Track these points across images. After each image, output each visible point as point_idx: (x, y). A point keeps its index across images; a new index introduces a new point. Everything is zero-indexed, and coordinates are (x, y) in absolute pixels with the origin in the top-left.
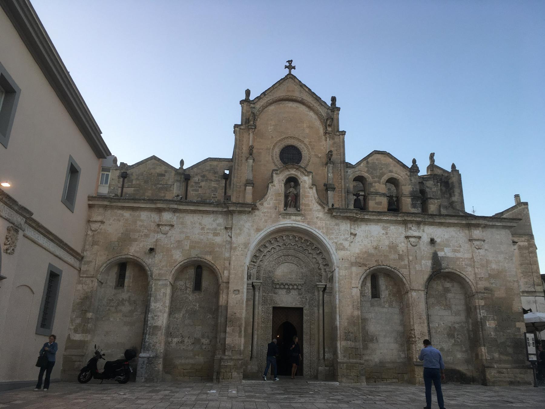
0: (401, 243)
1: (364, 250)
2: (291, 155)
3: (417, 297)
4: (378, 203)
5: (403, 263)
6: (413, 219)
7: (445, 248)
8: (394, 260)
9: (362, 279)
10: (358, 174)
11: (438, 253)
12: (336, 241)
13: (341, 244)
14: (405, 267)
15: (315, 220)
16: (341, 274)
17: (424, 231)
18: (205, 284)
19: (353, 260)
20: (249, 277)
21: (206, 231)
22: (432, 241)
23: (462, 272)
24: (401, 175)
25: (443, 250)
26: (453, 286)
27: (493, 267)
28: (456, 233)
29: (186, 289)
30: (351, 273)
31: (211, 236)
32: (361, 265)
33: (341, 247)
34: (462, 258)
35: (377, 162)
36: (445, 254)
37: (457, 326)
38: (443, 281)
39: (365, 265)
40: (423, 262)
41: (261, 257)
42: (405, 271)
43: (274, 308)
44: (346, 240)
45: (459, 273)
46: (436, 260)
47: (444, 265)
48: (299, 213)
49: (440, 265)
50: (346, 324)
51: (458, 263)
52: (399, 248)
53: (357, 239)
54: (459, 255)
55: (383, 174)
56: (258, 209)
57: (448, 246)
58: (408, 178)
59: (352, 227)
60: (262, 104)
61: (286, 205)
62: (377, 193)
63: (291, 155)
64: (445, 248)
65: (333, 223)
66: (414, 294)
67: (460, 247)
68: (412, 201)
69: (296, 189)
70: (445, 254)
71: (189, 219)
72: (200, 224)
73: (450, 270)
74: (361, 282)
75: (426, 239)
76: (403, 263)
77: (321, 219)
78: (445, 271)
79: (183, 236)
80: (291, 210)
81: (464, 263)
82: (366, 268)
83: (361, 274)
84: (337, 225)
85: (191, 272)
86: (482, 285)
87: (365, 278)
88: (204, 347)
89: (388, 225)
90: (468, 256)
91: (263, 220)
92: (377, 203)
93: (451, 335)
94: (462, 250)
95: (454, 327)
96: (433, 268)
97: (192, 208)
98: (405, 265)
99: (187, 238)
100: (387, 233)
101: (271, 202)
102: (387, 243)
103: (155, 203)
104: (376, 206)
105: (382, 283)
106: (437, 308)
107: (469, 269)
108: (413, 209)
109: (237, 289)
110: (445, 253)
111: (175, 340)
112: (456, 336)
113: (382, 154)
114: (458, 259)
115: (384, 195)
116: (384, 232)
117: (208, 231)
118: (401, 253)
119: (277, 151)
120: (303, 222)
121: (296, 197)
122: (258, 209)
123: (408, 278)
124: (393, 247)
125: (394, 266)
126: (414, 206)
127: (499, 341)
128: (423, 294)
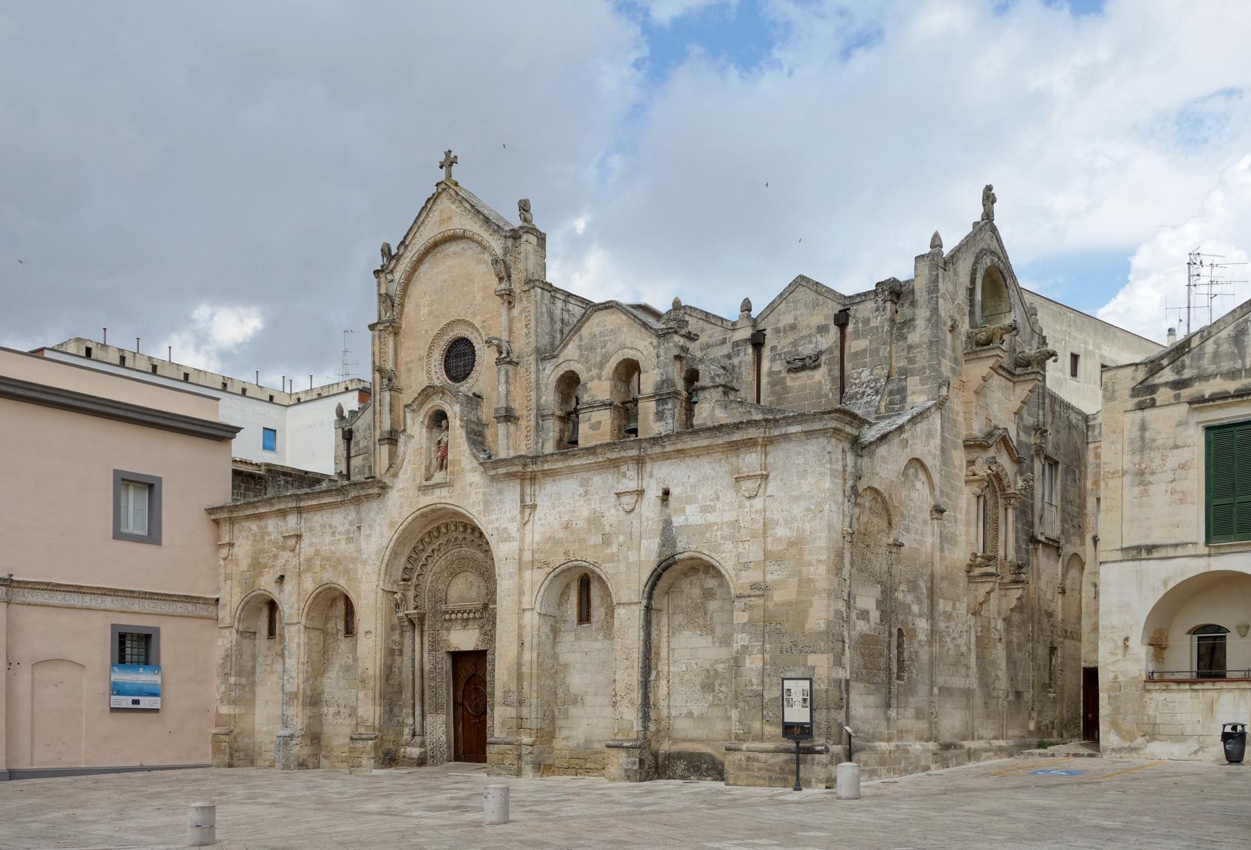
0: (609, 510)
1: (548, 534)
5: (609, 551)
6: (623, 454)
7: (688, 507)
8: (595, 546)
11: (673, 519)
12: (497, 525)
13: (505, 529)
14: (612, 559)
17: (651, 476)
22: (666, 493)
23: (713, 555)
24: (641, 346)
25: (683, 510)
27: (779, 534)
28: (713, 469)
31: (343, 545)
34: (716, 524)
35: (596, 330)
36: (686, 519)
38: (703, 576)
44: (513, 520)
45: (708, 559)
46: (667, 533)
47: (680, 546)
49: (675, 546)
51: (708, 535)
52: (605, 522)
53: (539, 513)
54: (711, 518)
55: (606, 358)
56: (389, 487)
57: (690, 500)
58: (654, 352)
59: (528, 491)
64: (688, 507)
65: (495, 491)
67: (718, 498)
68: (658, 405)
70: (686, 519)
71: (318, 519)
72: (330, 526)
73: (691, 554)
75: (653, 493)
76: (609, 551)
78: (681, 556)
81: (719, 533)
86: (753, 576)
89: (589, 475)
90: (729, 517)
92: (593, 427)
94: (719, 504)
96: (660, 554)
97: (314, 502)
98: (613, 554)
100: (586, 492)
102: (585, 513)
103: (257, 508)
104: (591, 431)
106: (687, 633)
107: (729, 546)
108: (659, 424)
110: (687, 516)
113: (607, 308)
114: (710, 526)
116: (581, 491)
118: (607, 529)
122: (389, 487)
124: (595, 521)
126: (660, 416)
127: (767, 696)
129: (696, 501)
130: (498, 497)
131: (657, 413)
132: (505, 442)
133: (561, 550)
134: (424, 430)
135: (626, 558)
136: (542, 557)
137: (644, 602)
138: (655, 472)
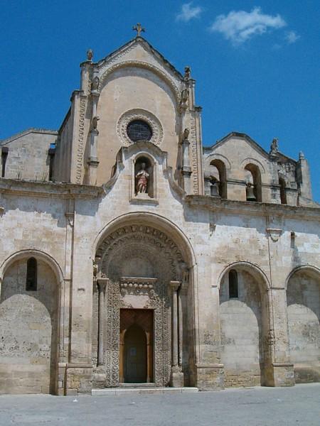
1: (224, 245)
2: (140, 128)
3: (277, 298)
4: (236, 193)
5: (263, 259)
7: (305, 244)
8: (254, 255)
9: (221, 277)
10: (215, 157)
15: (171, 209)
16: (199, 271)
17: (284, 225)
18: (40, 281)
19: (213, 255)
20: (95, 274)
21: (42, 218)
26: (309, 284)
29: (18, 287)
30: (211, 270)
32: (220, 261)
33: (200, 241)
36: (305, 249)
37: (312, 324)
38: (300, 278)
39: (225, 262)
40: (284, 258)
41: (107, 250)
42: (265, 269)
43: (121, 309)
44: (205, 232)
48: (152, 199)
50: (205, 326)
60: (107, 68)
61: (136, 191)
62: (237, 182)
63: (140, 128)
64: (305, 244)
66: (274, 292)
69: (147, 172)
74: (220, 280)
77: (177, 208)
79: (15, 223)
80: (143, 196)
82: (225, 264)
83: (220, 272)
84: (195, 215)
85: (24, 267)
87: (224, 276)
88: (42, 353)
91: (111, 206)
92: (235, 192)
93: (306, 334)
95: (309, 326)
96: (293, 265)
99: (20, 226)
101: (121, 186)
102: (247, 237)
105: (241, 281)
109: (83, 287)
111: (8, 345)
112: (310, 334)
115: (243, 183)
116: (244, 224)
117: (45, 218)
118: (262, 248)
119: (125, 124)
120: (157, 210)
121: (149, 181)
123: (268, 276)
124: (254, 242)
125: (254, 263)
126: (274, 196)
128: (283, 293)
129: (309, 242)
130: (194, 217)
131: (272, 195)
132: (190, 187)
133: (234, 255)
134: (133, 165)
135: (276, 264)
136: (221, 256)
137: (286, 288)
138: (286, 223)
